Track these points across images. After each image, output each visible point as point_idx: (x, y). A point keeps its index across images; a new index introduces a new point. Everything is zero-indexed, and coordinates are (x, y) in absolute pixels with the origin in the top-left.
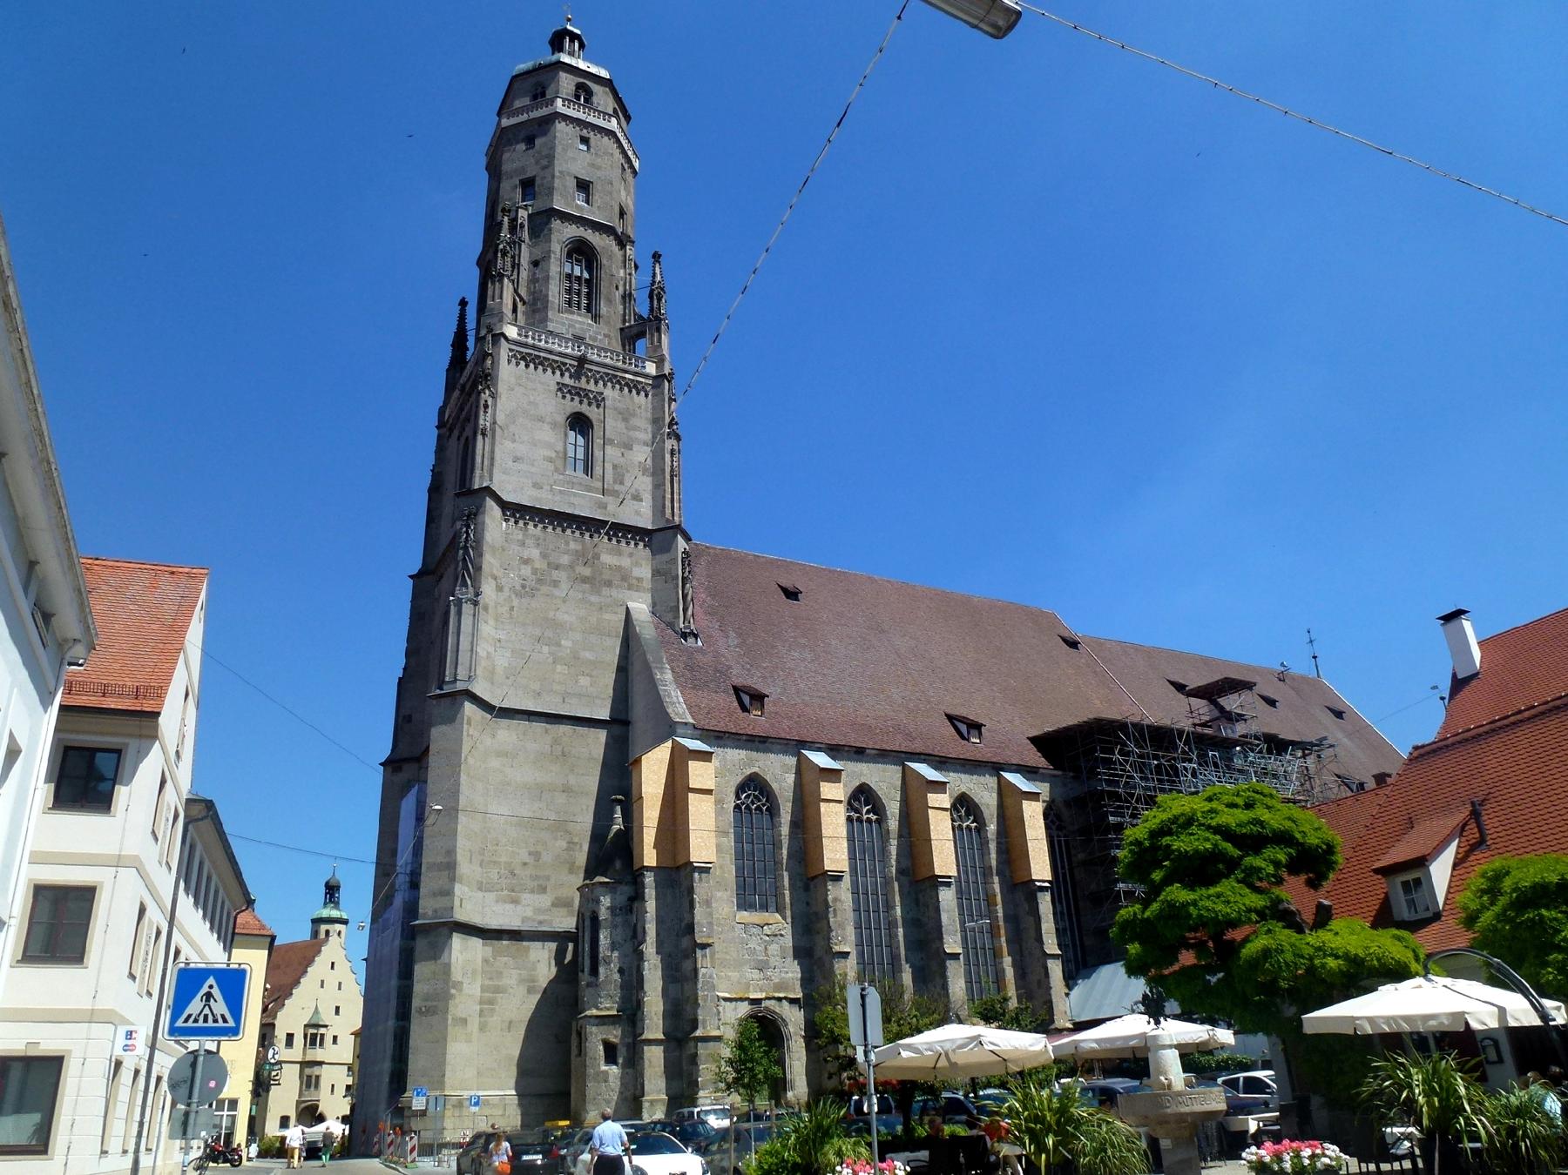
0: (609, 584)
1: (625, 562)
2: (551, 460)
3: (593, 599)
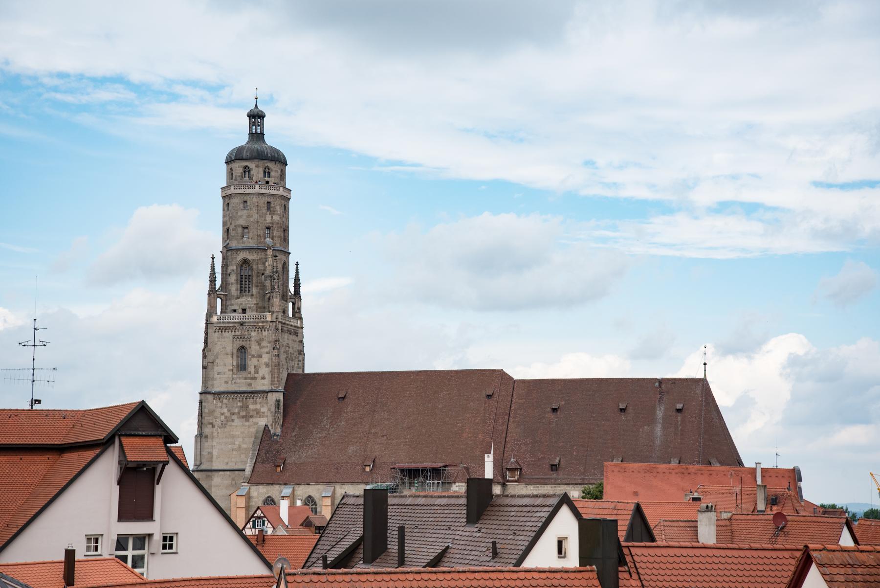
0: (252, 417)
1: (258, 406)
3: (247, 424)
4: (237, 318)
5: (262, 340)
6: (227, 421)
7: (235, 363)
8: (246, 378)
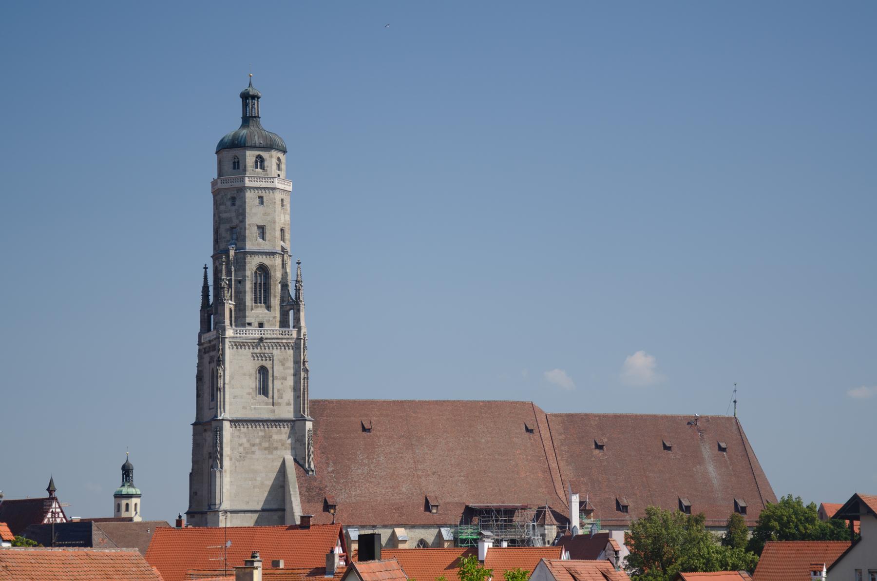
0: (276, 448)
2: (249, 394)
3: (270, 457)
4: (253, 333)
6: (247, 453)
7: (254, 386)
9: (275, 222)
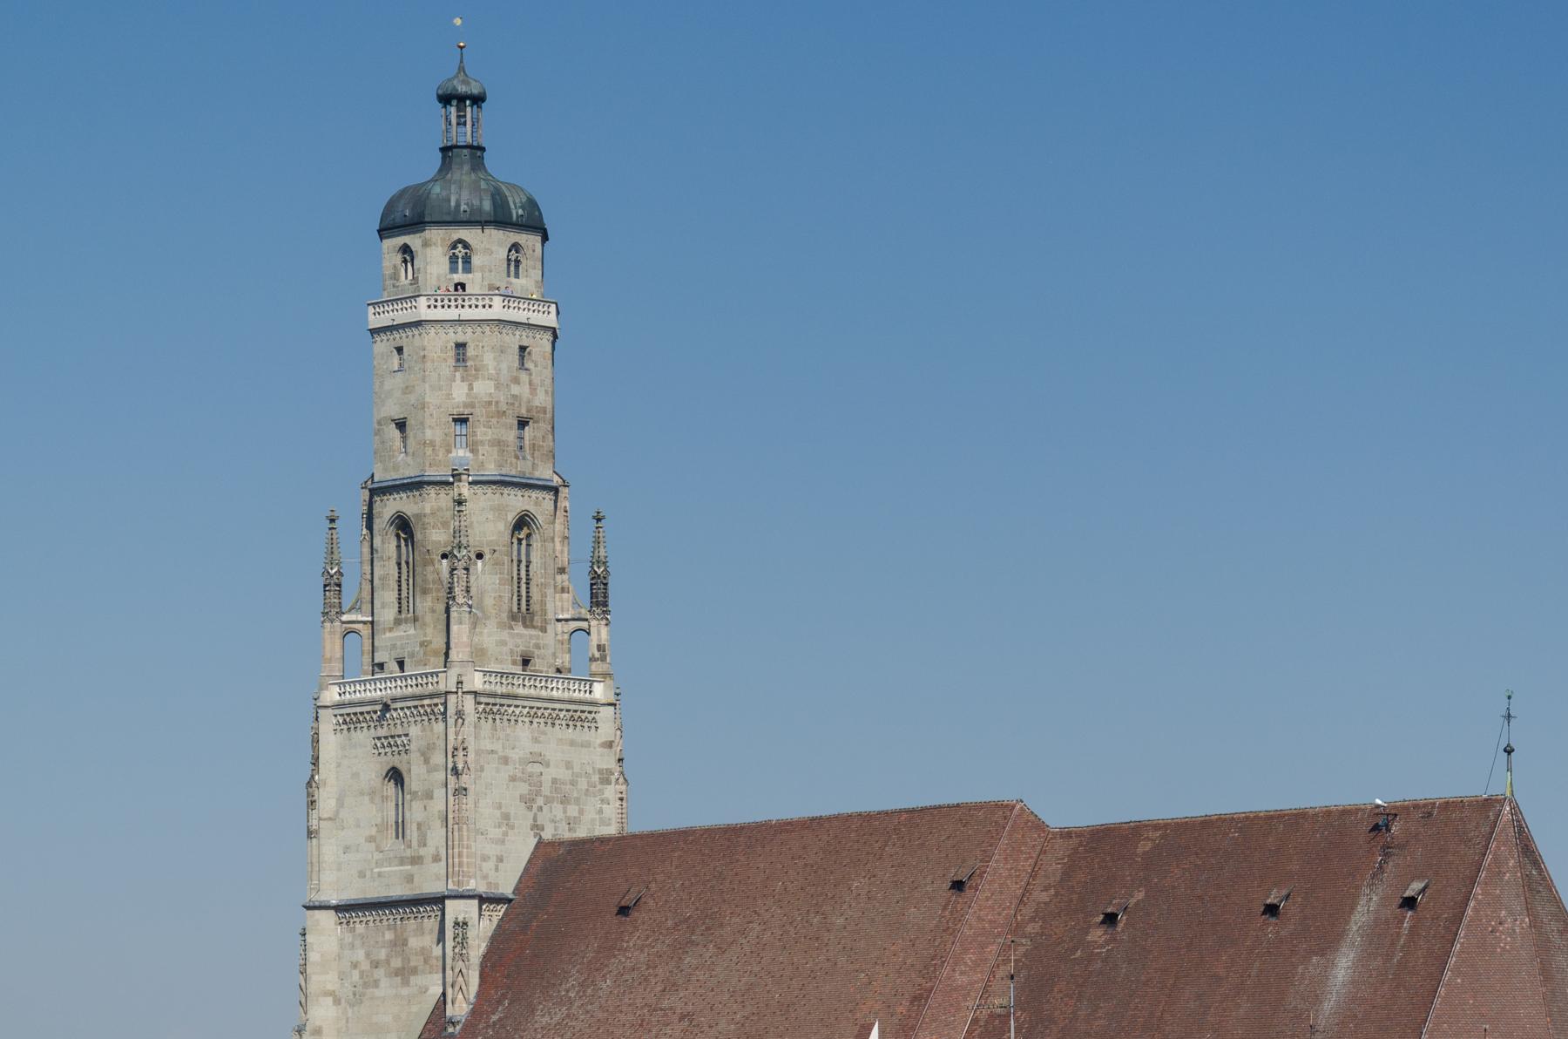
0: (414, 971)
3: (405, 991)
5: (431, 747)
8: (402, 862)
9: (423, 406)
